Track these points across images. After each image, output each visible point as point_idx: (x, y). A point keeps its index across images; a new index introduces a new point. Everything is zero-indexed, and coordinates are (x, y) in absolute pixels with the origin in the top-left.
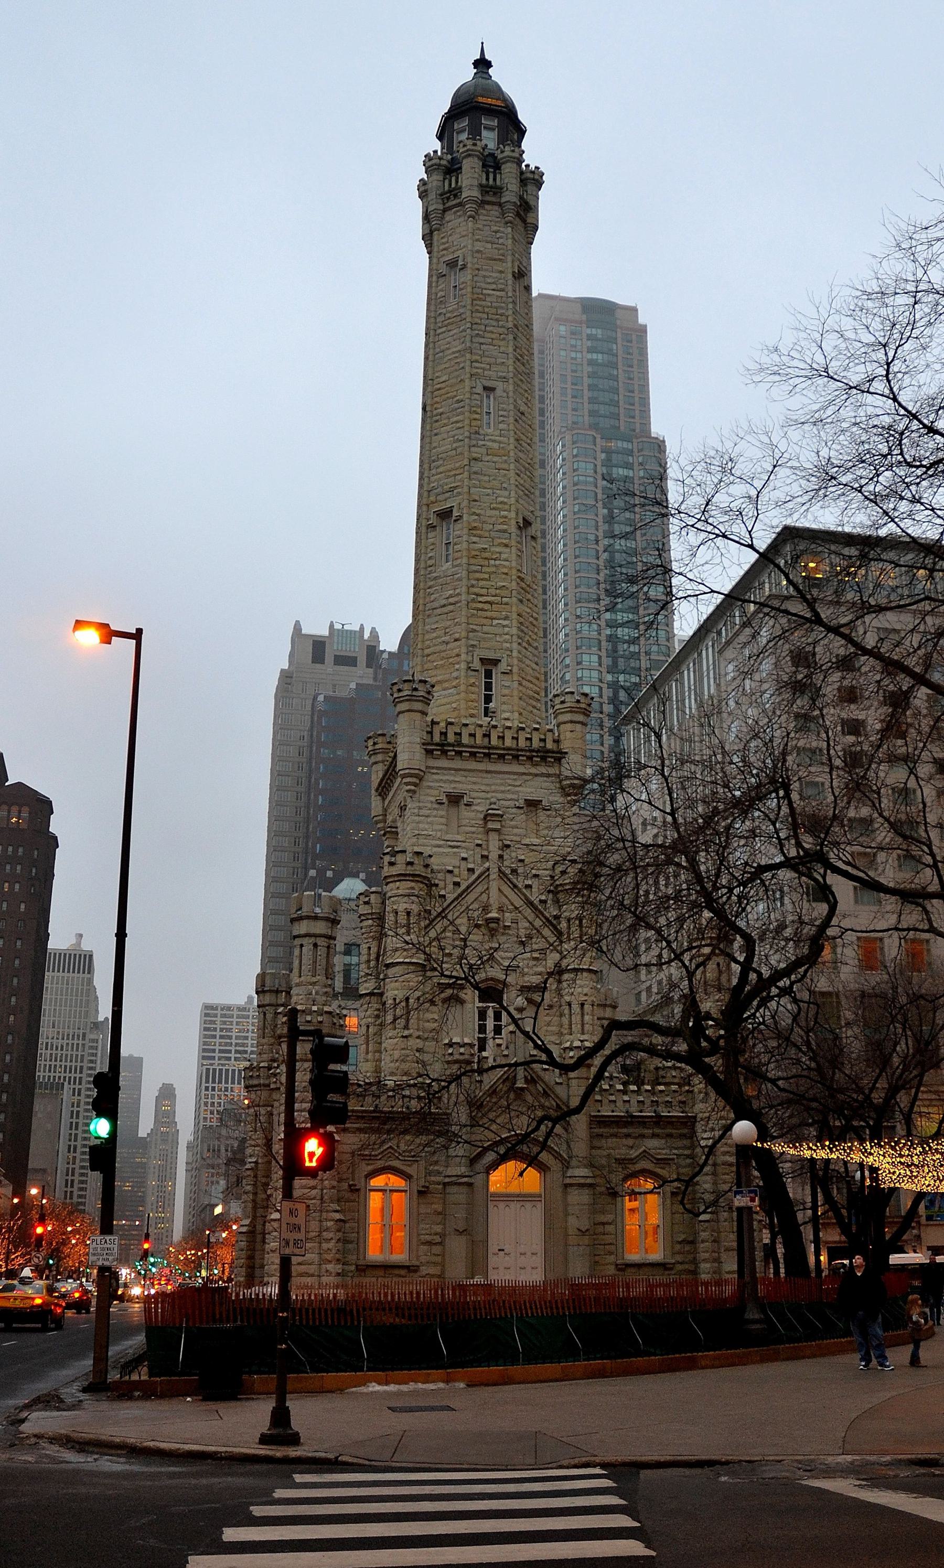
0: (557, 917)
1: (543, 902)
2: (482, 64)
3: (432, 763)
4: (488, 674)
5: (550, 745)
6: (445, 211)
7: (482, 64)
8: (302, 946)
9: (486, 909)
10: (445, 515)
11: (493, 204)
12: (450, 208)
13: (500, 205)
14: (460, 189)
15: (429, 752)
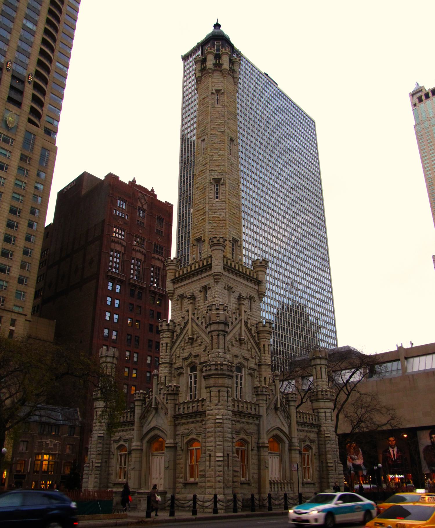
0: (259, 343)
1: (255, 336)
2: (217, 26)
3: (225, 273)
4: (233, 245)
5: (255, 277)
6: (215, 70)
7: (217, 26)
8: (218, 335)
9: (240, 335)
10: (217, 181)
11: (231, 75)
12: (217, 70)
13: (233, 78)
14: (222, 64)
15: (224, 268)
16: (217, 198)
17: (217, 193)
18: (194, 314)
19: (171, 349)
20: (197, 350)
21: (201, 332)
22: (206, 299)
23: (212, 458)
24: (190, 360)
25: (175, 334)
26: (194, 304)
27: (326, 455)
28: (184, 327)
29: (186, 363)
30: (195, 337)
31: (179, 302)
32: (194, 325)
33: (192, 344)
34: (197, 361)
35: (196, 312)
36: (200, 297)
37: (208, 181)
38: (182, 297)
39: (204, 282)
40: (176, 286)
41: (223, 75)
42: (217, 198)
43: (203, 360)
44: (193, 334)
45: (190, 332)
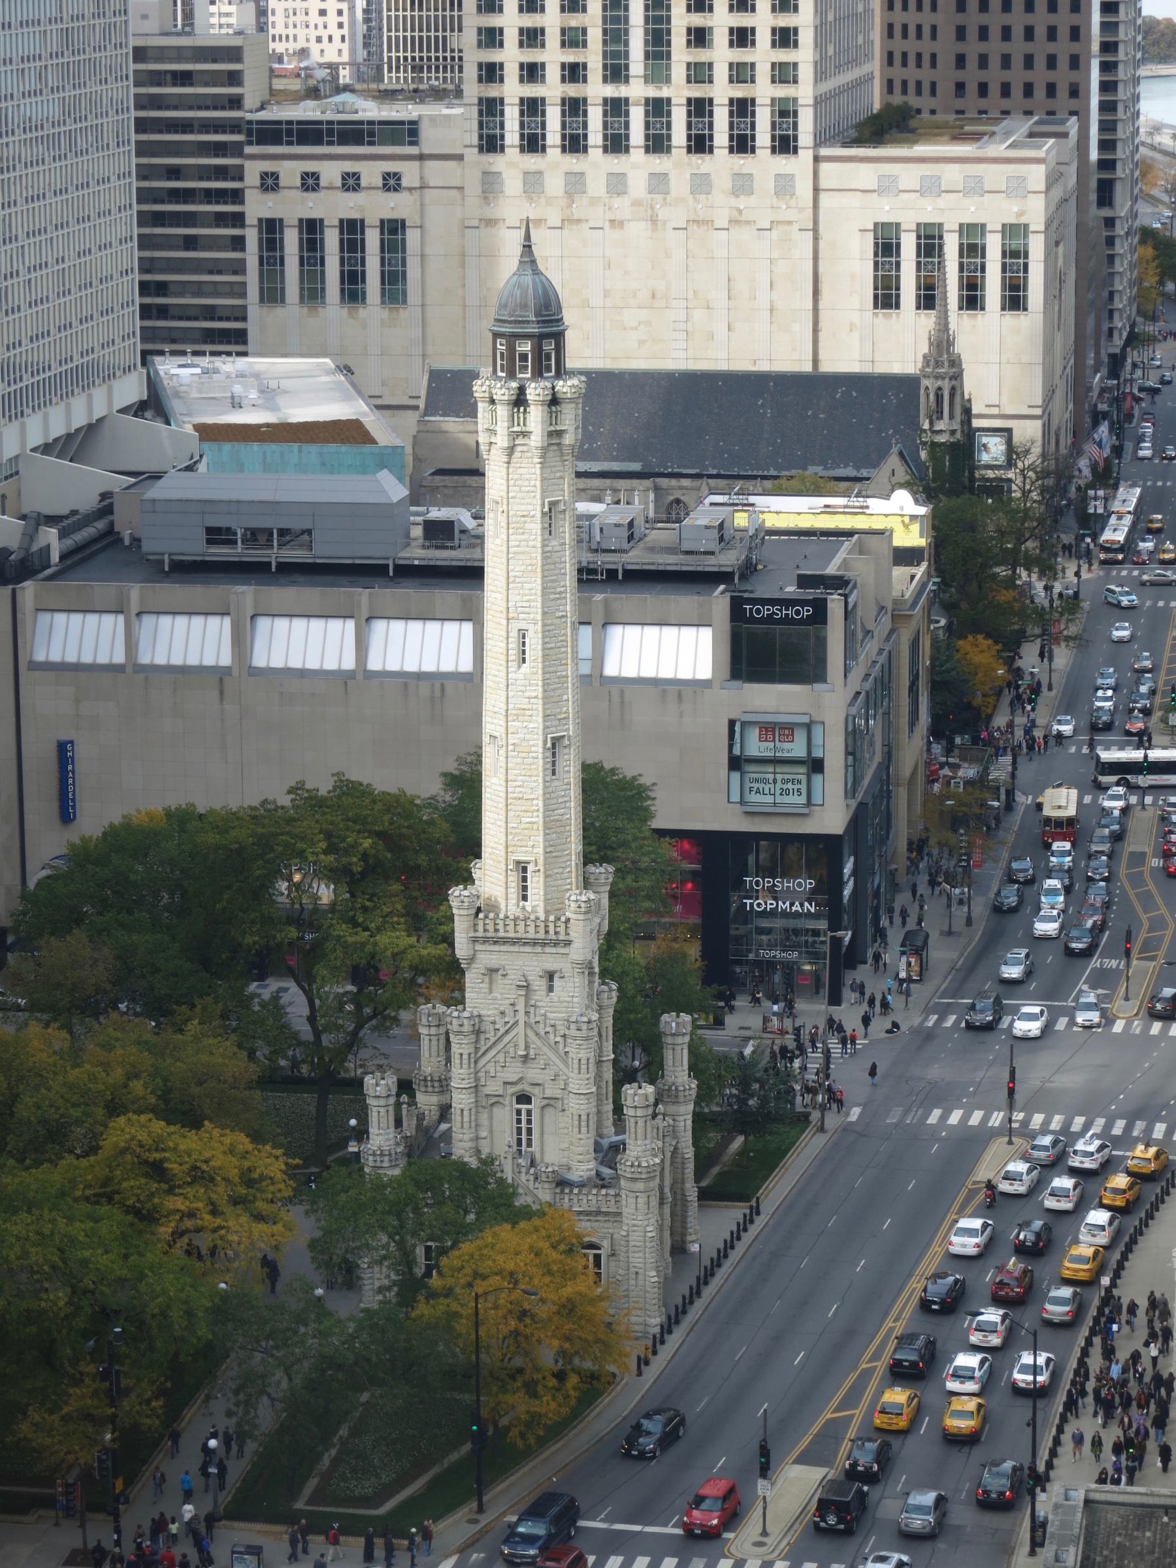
16: (554, 773)
17: (554, 763)
18: (527, 1013)
19: (476, 1062)
20: (533, 1073)
21: (546, 1049)
22: (551, 989)
23: (641, 1277)
24: (519, 1088)
25: (482, 1037)
26: (527, 997)
27: (683, 1182)
28: (507, 1032)
29: (512, 1090)
30: (532, 1052)
31: (487, 979)
32: (531, 1034)
33: (524, 1062)
34: (535, 1092)
35: (532, 1010)
36: (539, 984)
37: (540, 743)
38: (492, 971)
39: (551, 966)
40: (478, 947)
41: (562, 455)
42: (554, 773)
43: (548, 1093)
44: (527, 1047)
45: (522, 1045)
